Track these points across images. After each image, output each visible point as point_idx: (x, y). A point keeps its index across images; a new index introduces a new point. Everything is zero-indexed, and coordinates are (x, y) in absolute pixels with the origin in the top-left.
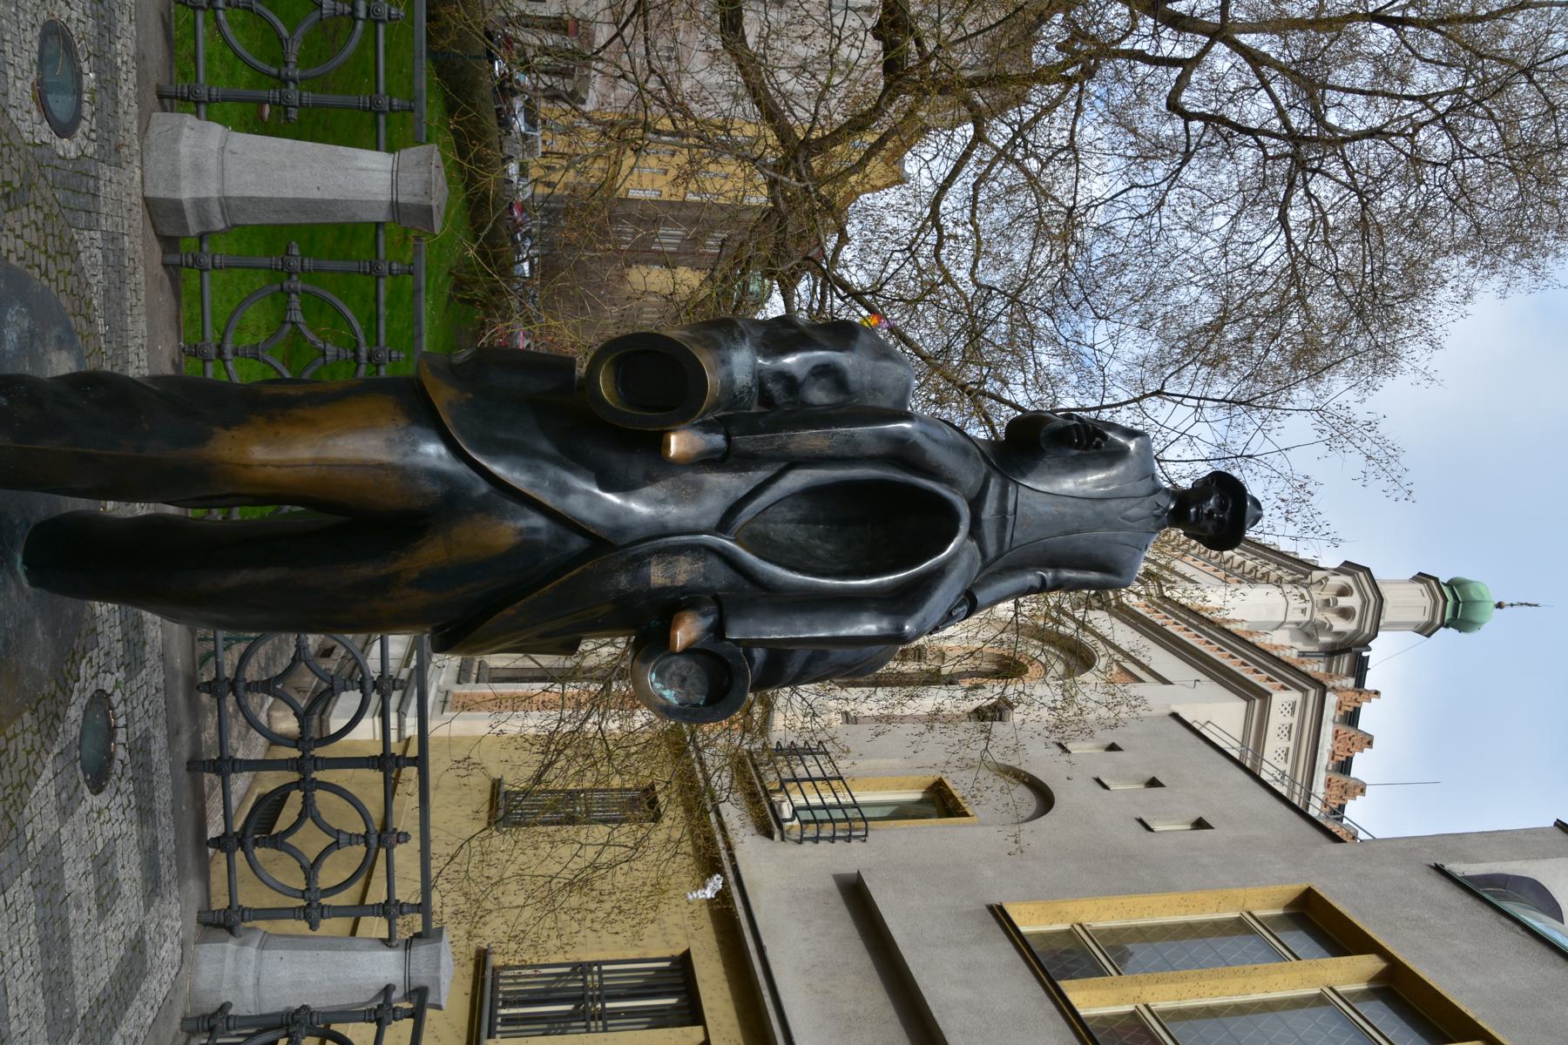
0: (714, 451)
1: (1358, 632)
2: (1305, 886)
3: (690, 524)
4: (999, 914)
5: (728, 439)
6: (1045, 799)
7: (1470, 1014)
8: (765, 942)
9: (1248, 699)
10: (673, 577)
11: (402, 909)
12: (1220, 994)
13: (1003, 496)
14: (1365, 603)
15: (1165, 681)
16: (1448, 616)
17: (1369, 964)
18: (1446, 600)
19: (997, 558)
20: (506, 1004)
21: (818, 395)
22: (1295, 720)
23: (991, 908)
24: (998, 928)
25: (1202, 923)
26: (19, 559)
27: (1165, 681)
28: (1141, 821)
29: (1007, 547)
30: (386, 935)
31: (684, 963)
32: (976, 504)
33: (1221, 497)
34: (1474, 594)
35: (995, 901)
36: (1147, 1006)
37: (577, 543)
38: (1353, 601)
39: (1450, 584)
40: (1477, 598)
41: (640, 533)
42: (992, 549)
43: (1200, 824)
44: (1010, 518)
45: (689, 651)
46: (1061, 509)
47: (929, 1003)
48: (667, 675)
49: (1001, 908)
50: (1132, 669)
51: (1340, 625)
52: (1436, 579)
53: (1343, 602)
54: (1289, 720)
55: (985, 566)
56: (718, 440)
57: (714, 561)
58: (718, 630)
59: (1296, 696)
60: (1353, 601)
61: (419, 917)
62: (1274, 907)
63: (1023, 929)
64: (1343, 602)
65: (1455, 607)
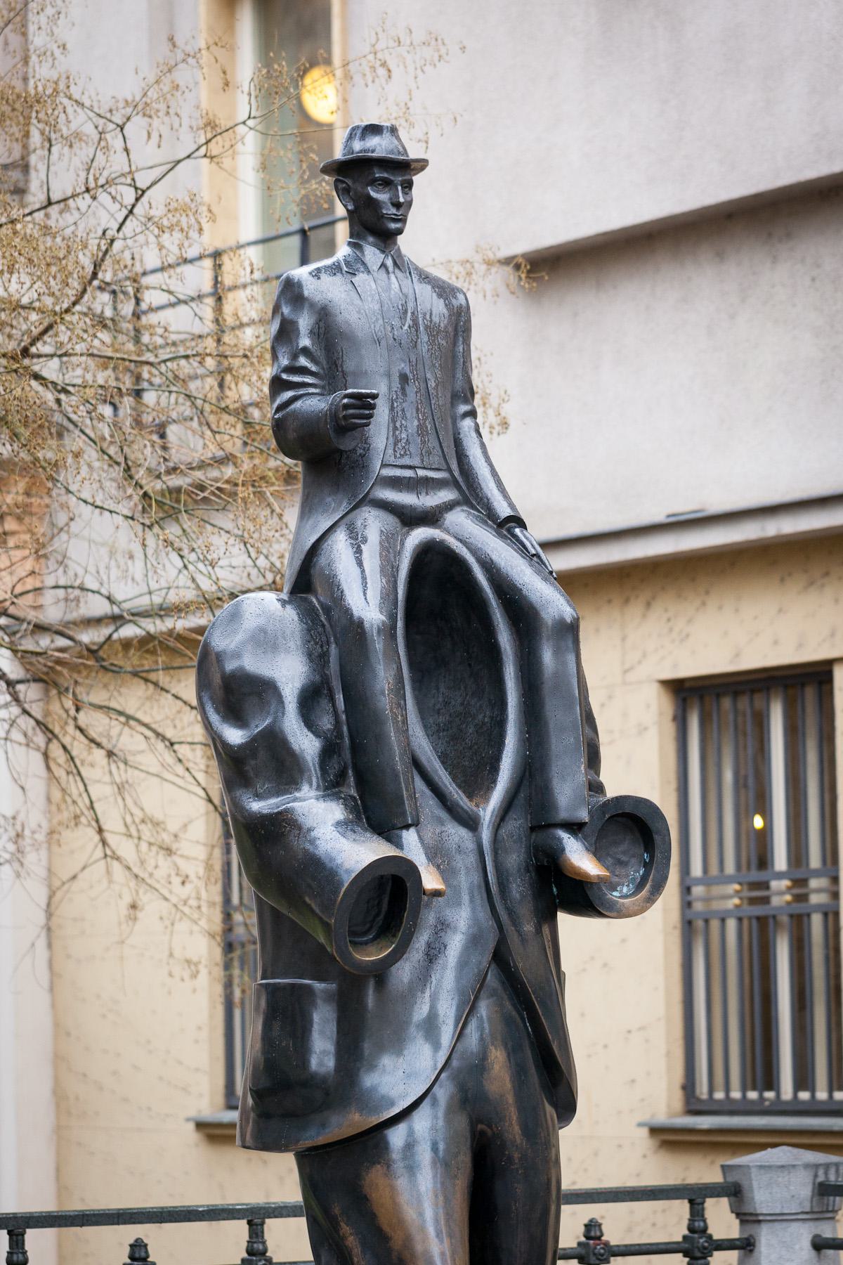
3: (472, 859)
5: (407, 827)
8: (657, 515)
11: (697, 1226)
20: (770, 1081)
21: (326, 723)
30: (733, 1255)
31: (687, 693)
32: (410, 519)
33: (373, 182)
37: (492, 980)
41: (484, 914)
42: (446, 495)
44: (421, 473)
57: (503, 832)
58: (575, 828)
61: (710, 1203)
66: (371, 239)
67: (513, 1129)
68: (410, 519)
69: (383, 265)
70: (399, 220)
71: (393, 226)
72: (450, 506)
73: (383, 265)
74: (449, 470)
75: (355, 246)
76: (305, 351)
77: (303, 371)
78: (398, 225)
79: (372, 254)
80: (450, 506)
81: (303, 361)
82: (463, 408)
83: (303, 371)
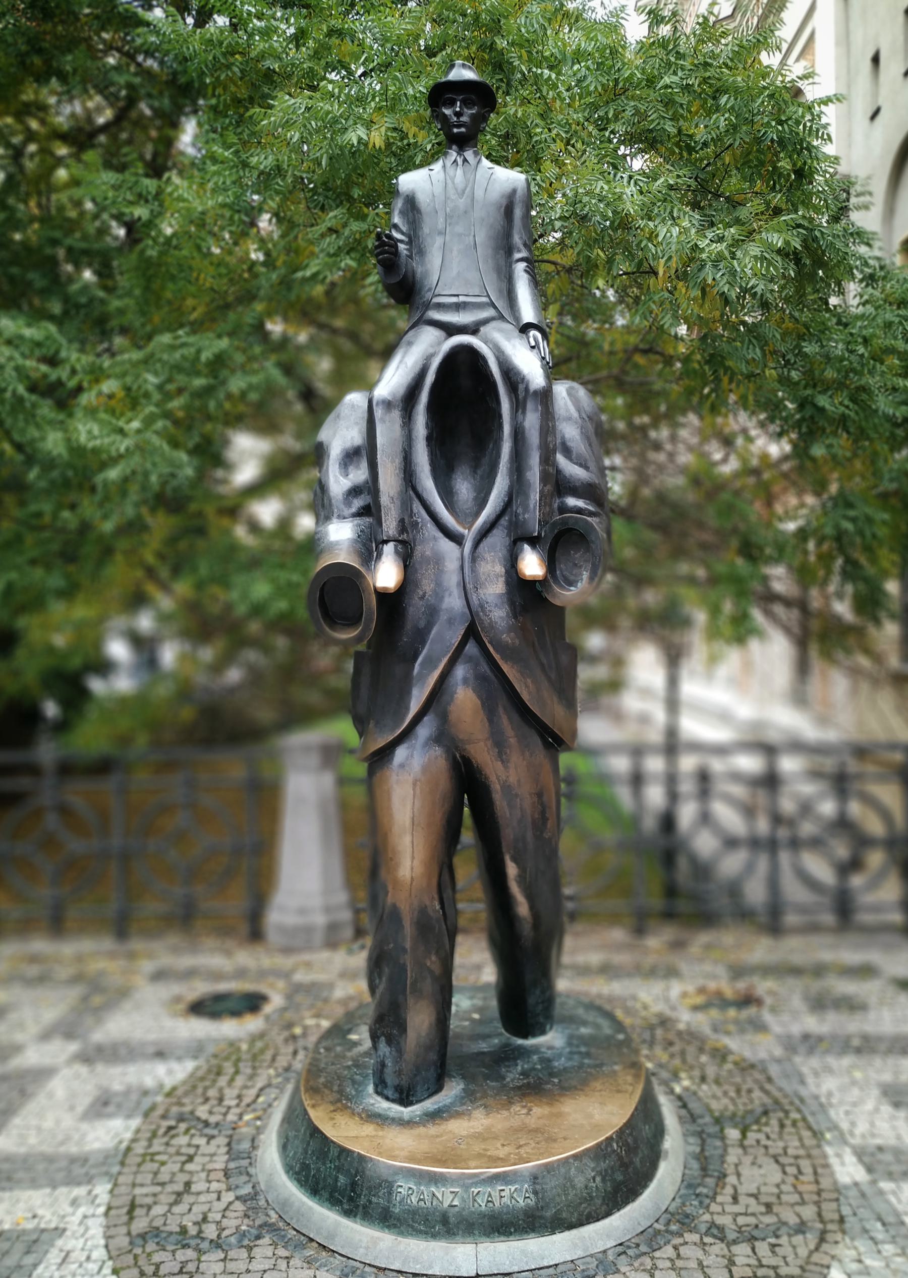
0: (397, 552)
5: (386, 542)
10: (497, 576)
13: (440, 307)
19: (495, 307)
21: (359, 474)
26: (520, 1041)
29: (485, 299)
32: (450, 330)
37: (471, 648)
44: (462, 299)
45: (551, 563)
46: (455, 253)
48: (572, 578)
55: (501, 317)
56: (389, 548)
58: (534, 542)
66: (454, 147)
67: (483, 754)
68: (450, 330)
70: (458, 126)
71: (455, 130)
72: (485, 322)
73: (455, 161)
74: (488, 296)
78: (463, 130)
80: (485, 322)
82: (517, 256)
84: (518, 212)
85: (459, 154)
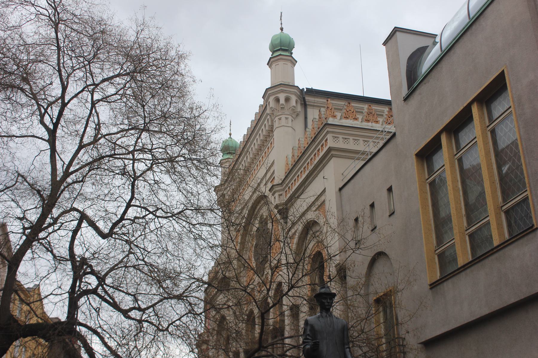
1: (295, 95)
2: (414, 156)
4: (434, 286)
6: (380, 255)
7: (462, 108)
9: (333, 156)
12: (460, 200)
14: (283, 91)
15: (324, 191)
16: (287, 54)
17: (444, 139)
18: (280, 55)
22: (341, 136)
23: (431, 289)
24: (438, 287)
25: (432, 199)
27: (324, 191)
28: (390, 216)
34: (278, 42)
35: (429, 287)
36: (466, 230)
38: (282, 97)
39: (273, 52)
40: (279, 40)
43: (390, 190)
47: (470, 320)
49: (430, 285)
50: (319, 204)
51: (293, 102)
52: (270, 58)
53: (282, 101)
54: (341, 140)
59: (329, 137)
60: (282, 97)
62: (424, 169)
63: (438, 278)
64: (282, 101)
65: (282, 50)
69: (326, 316)
70: (328, 306)
73: (326, 316)
75: (321, 312)
76: (308, 335)
77: (308, 339)
79: (324, 314)
81: (308, 337)
82: (346, 346)
83: (308, 339)
84: (345, 333)
85: (327, 313)
